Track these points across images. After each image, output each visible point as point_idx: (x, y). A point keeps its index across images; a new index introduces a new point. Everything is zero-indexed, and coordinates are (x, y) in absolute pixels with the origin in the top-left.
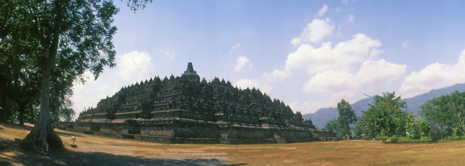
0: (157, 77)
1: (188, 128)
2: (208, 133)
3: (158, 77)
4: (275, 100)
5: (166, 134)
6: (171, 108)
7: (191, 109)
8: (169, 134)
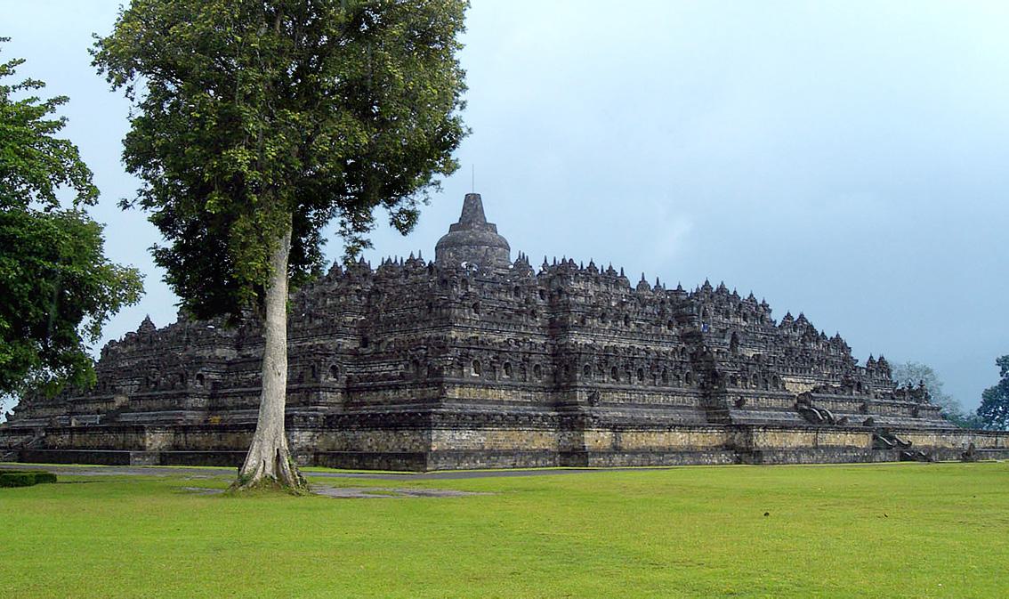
2: (527, 440)
4: (788, 316)
8: (418, 447)
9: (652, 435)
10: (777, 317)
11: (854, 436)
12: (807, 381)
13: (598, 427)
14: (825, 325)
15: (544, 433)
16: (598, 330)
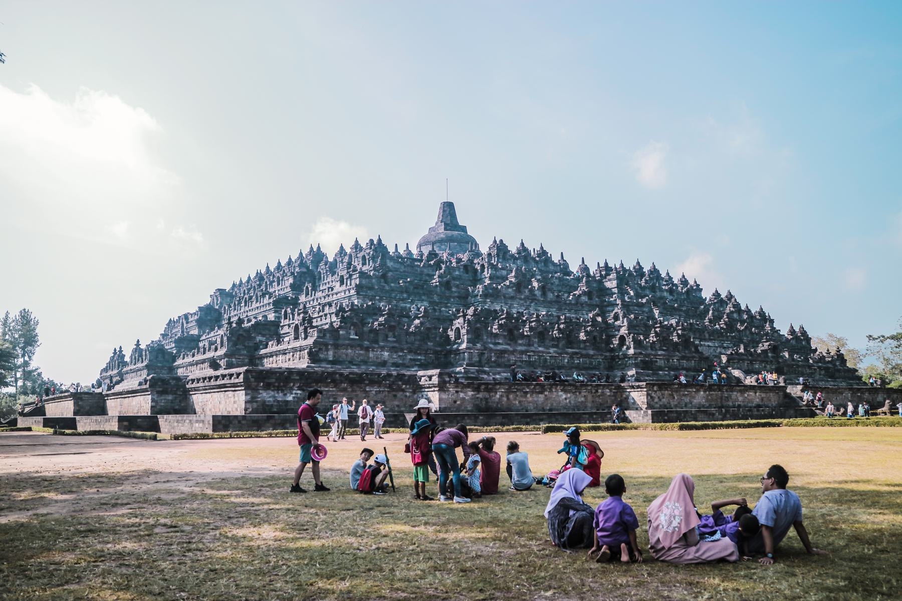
0: (315, 250)
1: (299, 392)
3: (319, 248)
4: (717, 294)
5: (232, 409)
6: (296, 338)
7: (357, 337)
9: (529, 396)
10: (707, 294)
11: (763, 395)
12: (725, 345)
13: (457, 387)
14: (750, 302)
15: (400, 394)
16: (512, 298)
